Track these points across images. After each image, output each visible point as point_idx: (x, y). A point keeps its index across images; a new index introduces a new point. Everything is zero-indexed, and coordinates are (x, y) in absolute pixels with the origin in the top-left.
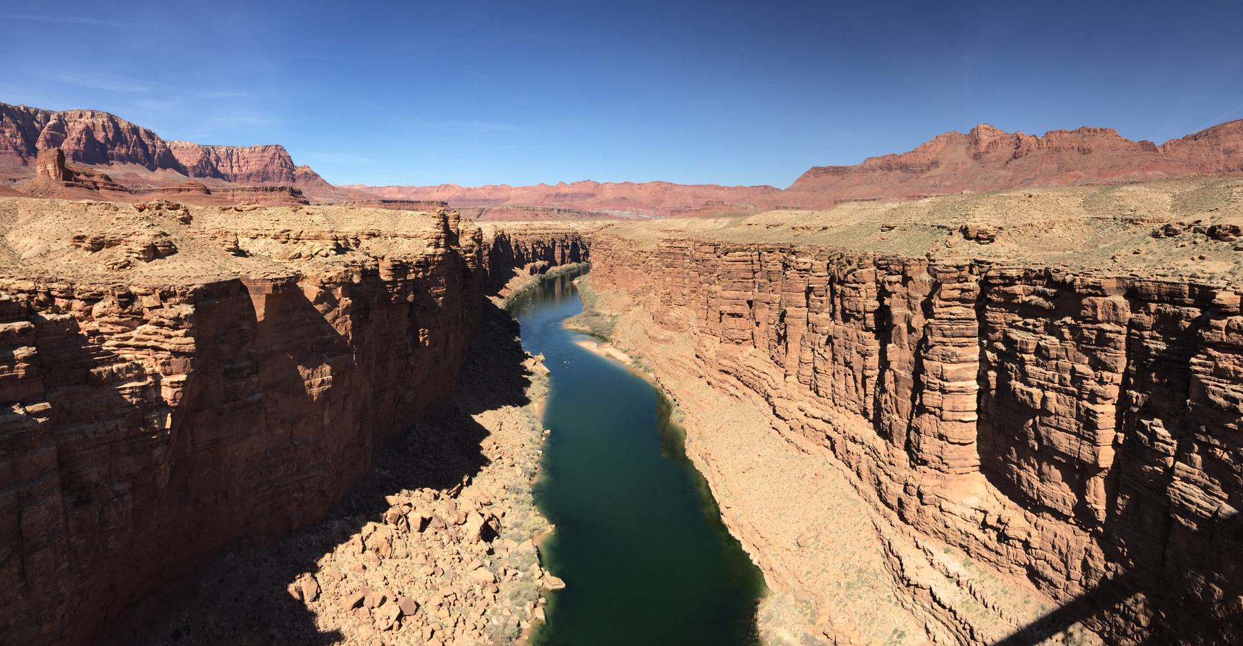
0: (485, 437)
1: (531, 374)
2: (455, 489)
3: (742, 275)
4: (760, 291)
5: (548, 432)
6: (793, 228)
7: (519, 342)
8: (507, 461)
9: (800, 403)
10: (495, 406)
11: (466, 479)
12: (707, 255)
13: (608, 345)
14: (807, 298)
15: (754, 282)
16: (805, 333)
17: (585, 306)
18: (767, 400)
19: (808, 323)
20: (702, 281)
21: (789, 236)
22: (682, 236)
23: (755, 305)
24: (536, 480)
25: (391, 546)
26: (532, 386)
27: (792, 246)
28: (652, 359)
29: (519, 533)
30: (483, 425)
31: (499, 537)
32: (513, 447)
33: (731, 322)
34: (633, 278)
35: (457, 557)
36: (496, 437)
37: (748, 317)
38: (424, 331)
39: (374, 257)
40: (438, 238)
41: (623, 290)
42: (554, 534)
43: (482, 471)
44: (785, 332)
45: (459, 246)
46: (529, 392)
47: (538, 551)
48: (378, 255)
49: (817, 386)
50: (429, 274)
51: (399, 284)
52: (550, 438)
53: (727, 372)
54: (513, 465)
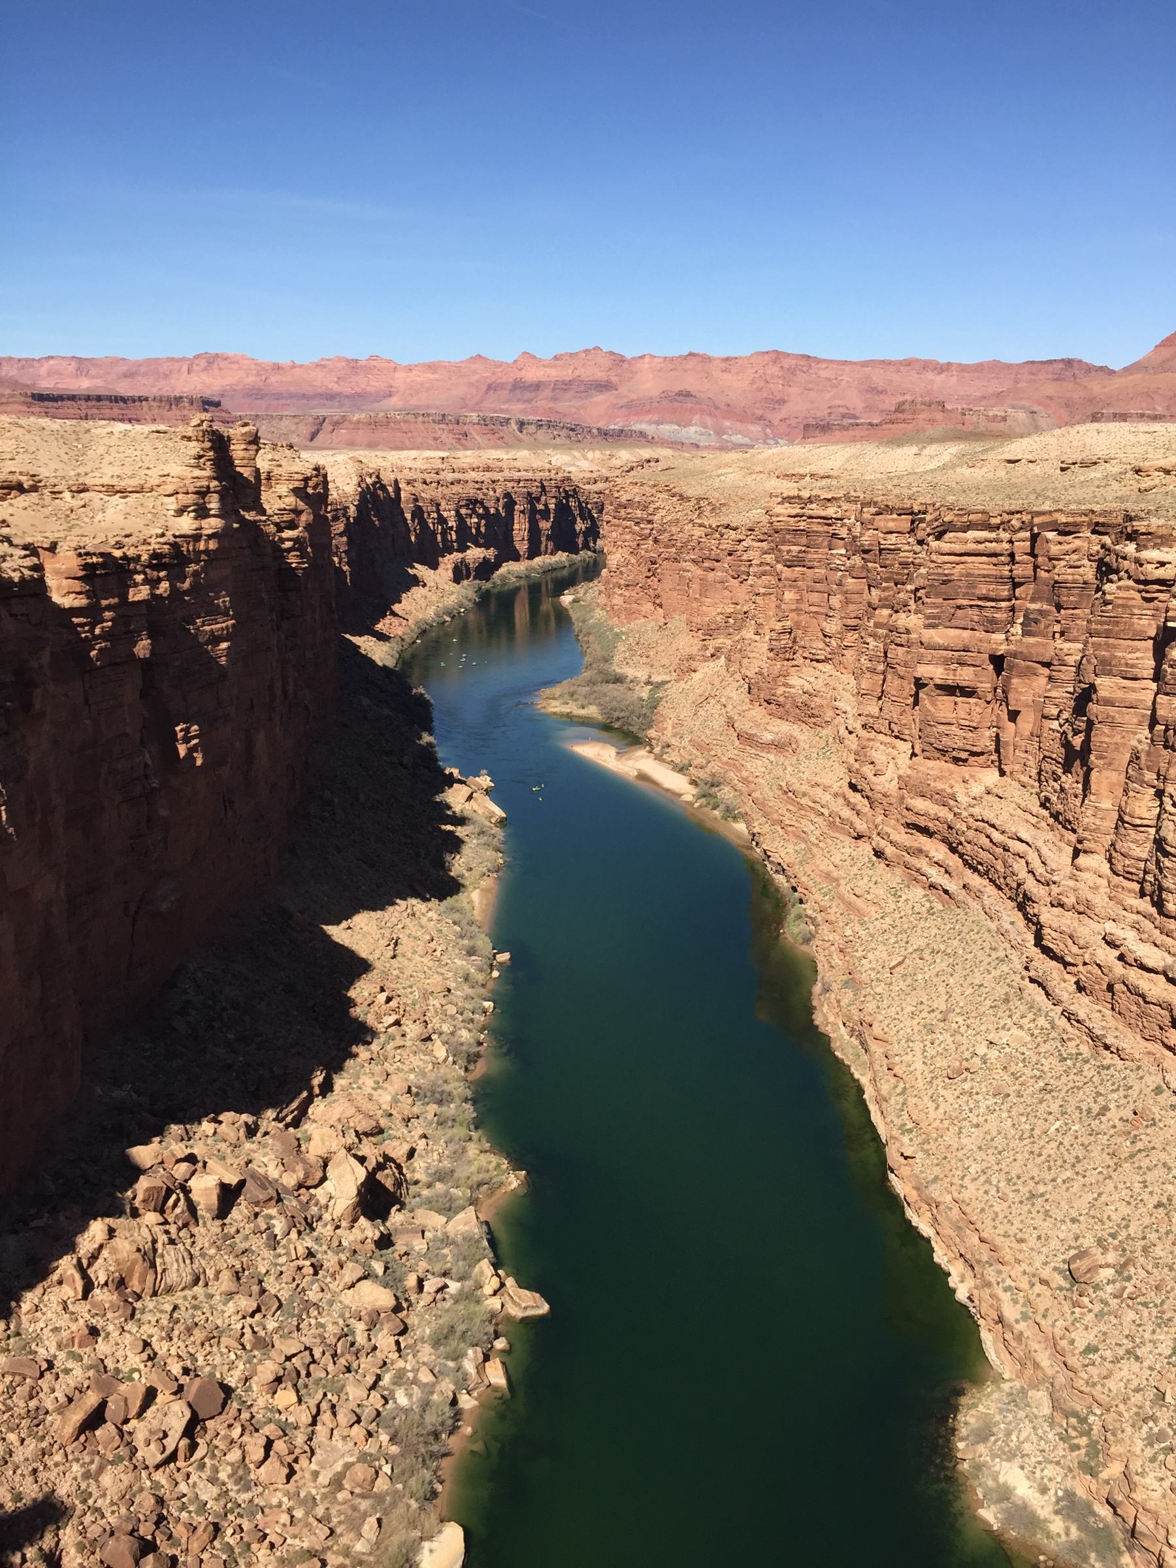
0: (359, 976)
1: (461, 821)
2: (295, 1105)
3: (983, 590)
4: (1025, 633)
5: (504, 957)
6: (1138, 471)
7: (430, 745)
8: (413, 1030)
9: (1109, 927)
10: (378, 902)
11: (318, 1079)
12: (892, 538)
13: (642, 752)
14: (1159, 655)
15: (1013, 609)
16: (1144, 747)
17: (588, 659)
18: (1021, 907)
19: (1153, 722)
20: (875, 601)
21: (1124, 491)
22: (829, 488)
23: (1011, 668)
24: (480, 1069)
25: (153, 1265)
26: (466, 850)
27: (1129, 518)
28: (745, 789)
29: (447, 1192)
30: (354, 948)
31: (403, 1206)
32: (426, 995)
33: (944, 707)
34: (704, 592)
35: (308, 1263)
36: (385, 974)
37: (990, 697)
38: (187, 730)
39: (25, 547)
40: (203, 493)
41: (678, 622)
42: (523, 1191)
43: (356, 1056)
44: (1087, 743)
45: (263, 512)
46: (458, 865)
47: (490, 1232)
48: (37, 539)
49: (1161, 888)
50: (187, 585)
51: (108, 615)
52: (509, 970)
53: (925, 831)
54: (429, 1039)
